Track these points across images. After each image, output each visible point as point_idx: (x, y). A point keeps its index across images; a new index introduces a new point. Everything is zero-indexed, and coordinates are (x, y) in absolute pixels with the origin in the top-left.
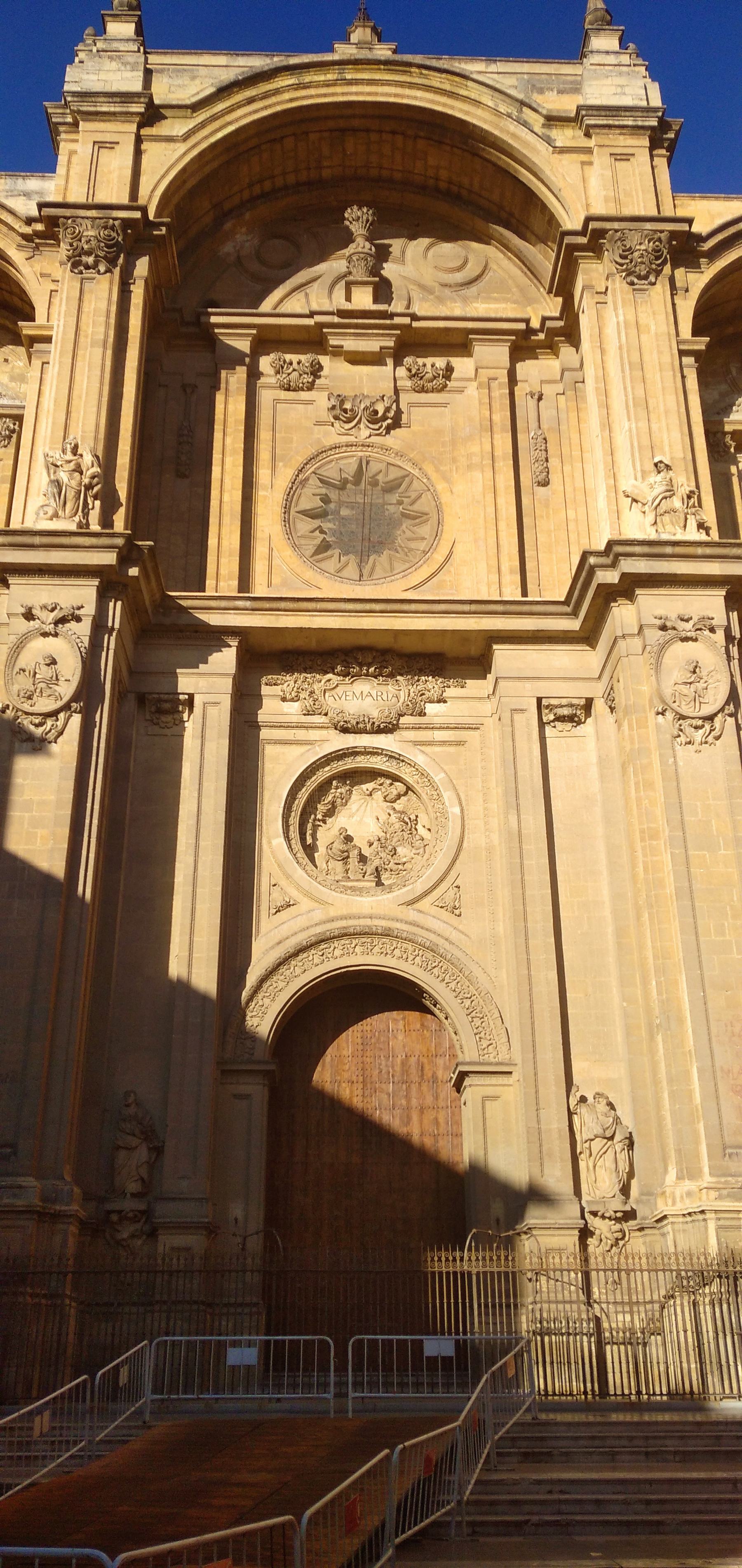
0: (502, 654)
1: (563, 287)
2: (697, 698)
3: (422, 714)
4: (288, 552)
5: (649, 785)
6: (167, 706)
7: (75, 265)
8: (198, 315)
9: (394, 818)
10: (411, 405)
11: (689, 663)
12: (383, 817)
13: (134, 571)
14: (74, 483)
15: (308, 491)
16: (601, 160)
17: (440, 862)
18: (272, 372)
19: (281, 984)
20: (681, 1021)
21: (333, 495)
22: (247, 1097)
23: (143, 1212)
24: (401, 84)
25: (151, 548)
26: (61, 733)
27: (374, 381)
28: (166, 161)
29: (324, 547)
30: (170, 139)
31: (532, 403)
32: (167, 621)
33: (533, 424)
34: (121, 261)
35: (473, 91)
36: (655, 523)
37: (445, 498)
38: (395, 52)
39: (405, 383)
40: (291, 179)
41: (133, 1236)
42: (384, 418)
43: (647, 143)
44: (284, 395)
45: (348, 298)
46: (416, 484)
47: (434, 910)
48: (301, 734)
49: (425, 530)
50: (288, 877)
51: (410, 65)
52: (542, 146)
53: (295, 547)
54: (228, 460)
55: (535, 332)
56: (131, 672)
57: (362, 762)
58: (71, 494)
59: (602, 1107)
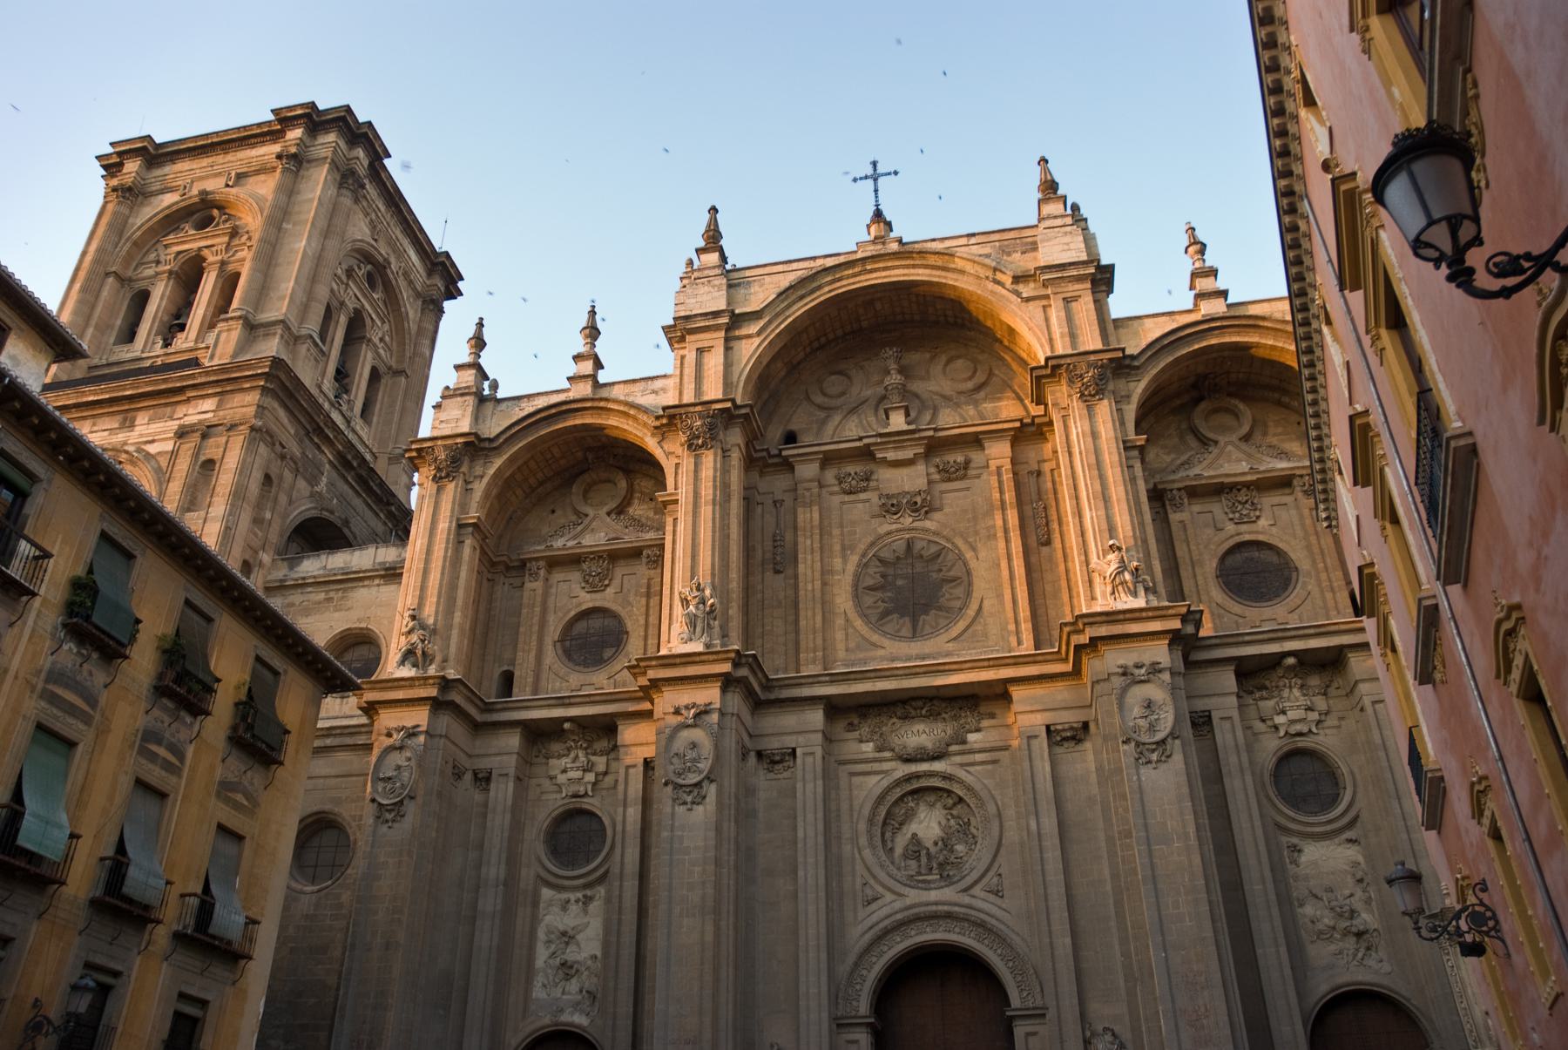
0: (1017, 692)
1: (1039, 400)
2: (1152, 728)
3: (964, 742)
4: (859, 623)
5: (1124, 797)
7: (690, 447)
9: (952, 822)
10: (942, 492)
12: (944, 822)
14: (699, 613)
15: (871, 571)
18: (835, 482)
20: (1151, 975)
21: (891, 571)
22: (856, 1042)
24: (907, 267)
25: (754, 656)
27: (912, 479)
29: (885, 614)
30: (749, 336)
31: (1033, 479)
32: (772, 696)
33: (1034, 497)
34: (721, 436)
35: (959, 264)
37: (973, 564)
39: (936, 477)
40: (840, 333)
44: (847, 498)
46: (950, 556)
47: (983, 894)
48: (876, 766)
49: (959, 591)
50: (874, 877)
52: (1013, 297)
53: (864, 616)
56: (751, 736)
57: (924, 783)
59: (1108, 1037)
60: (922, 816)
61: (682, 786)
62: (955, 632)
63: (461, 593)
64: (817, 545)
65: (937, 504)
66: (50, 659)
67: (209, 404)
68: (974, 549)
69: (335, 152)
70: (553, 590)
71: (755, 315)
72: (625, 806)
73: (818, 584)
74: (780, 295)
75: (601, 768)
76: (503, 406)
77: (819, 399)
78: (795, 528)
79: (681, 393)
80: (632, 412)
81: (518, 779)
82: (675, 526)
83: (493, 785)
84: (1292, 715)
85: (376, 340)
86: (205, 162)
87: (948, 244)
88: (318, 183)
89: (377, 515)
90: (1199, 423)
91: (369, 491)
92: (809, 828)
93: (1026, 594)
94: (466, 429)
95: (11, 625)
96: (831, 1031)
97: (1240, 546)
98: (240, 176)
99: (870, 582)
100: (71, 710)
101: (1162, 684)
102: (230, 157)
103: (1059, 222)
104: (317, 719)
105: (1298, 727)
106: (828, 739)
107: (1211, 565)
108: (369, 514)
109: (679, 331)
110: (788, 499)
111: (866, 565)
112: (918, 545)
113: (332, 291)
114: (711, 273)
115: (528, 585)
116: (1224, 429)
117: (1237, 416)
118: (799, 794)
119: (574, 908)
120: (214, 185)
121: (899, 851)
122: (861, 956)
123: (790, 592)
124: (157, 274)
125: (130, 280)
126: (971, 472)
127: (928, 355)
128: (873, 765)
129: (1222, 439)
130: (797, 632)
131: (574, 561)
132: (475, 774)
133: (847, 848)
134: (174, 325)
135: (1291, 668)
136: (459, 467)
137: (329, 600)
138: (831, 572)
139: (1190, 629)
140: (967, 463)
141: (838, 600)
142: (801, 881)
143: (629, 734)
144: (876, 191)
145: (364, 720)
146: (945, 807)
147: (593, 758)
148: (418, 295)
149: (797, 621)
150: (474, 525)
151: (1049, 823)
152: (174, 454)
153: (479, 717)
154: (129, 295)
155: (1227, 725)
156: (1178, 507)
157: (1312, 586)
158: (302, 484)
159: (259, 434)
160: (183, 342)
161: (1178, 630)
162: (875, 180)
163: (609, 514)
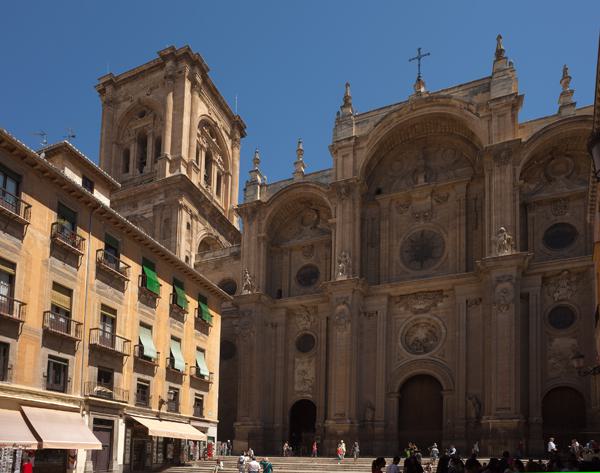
4: (401, 265)
37: (446, 239)
39: (434, 203)
62: (436, 266)
63: (261, 263)
67: (162, 197)
68: (447, 233)
78: (379, 230)
97: (556, 225)
100: (148, 315)
106: (388, 306)
107: (541, 234)
120: (142, 94)
128: (404, 316)
132: (272, 324)
150: (264, 238)
151: (463, 333)
158: (200, 225)
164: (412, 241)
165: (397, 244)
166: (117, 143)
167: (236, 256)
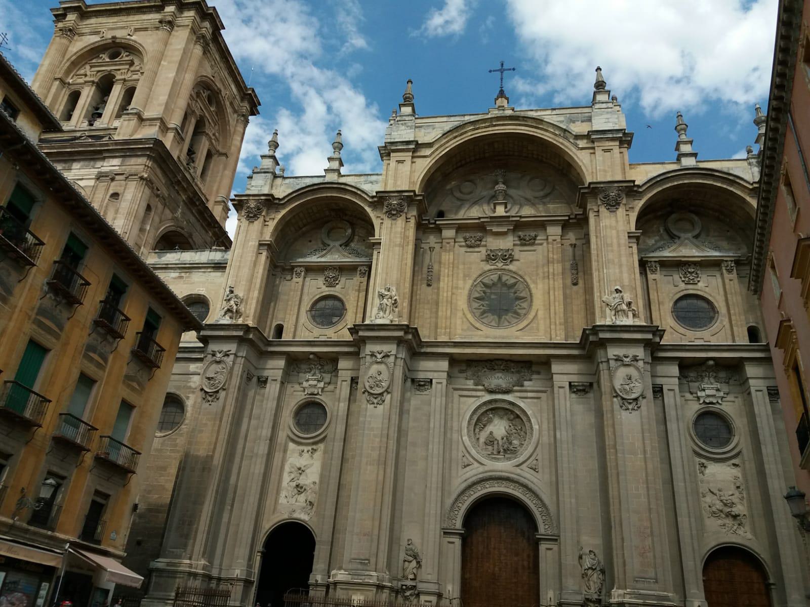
1: (583, 206)
3: (522, 386)
4: (469, 316)
6: (422, 383)
8: (436, 221)
10: (521, 251)
11: (627, 376)
12: (507, 427)
13: (410, 337)
16: (599, 152)
17: (530, 449)
19: (466, 498)
20: (621, 525)
21: (488, 291)
22: (453, 543)
23: (415, 586)
25: (416, 329)
26: (384, 401)
27: (507, 243)
28: (423, 166)
31: (570, 249)
32: (423, 350)
34: (406, 210)
36: (615, 315)
37: (534, 291)
38: (513, 110)
39: (518, 242)
40: (473, 158)
41: (411, 595)
42: (509, 258)
43: (617, 143)
45: (495, 208)
48: (474, 393)
49: (525, 305)
51: (519, 117)
54: (446, 279)
55: (572, 219)
58: (388, 307)
59: (592, 556)
60: (496, 422)
61: (373, 394)
63: (258, 281)
64: (451, 273)
65: (516, 257)
66: (40, 301)
67: (116, 162)
68: (535, 283)
69: (193, 22)
70: (307, 284)
71: (429, 145)
72: (339, 401)
73: (450, 293)
74: (443, 135)
75: (327, 380)
76: (287, 181)
77: (458, 195)
78: (440, 263)
79: (386, 185)
80: (359, 192)
81: (282, 383)
82: (378, 256)
83: (268, 385)
84: (708, 392)
85: (211, 135)
86: (115, 19)
87: (539, 113)
88: (181, 38)
89: (207, 232)
90: (670, 225)
91: (204, 219)
92: (436, 422)
93: (562, 310)
94: (266, 192)
95: (20, 281)
96: (440, 536)
98: (136, 30)
99: (477, 295)
101: (637, 369)
102: (131, 18)
103: (604, 106)
104: (179, 342)
105: (711, 399)
106: (450, 376)
107: (668, 305)
108: (204, 232)
109: (387, 151)
110: (437, 246)
111: (475, 286)
112: (504, 278)
113: (188, 104)
114: (407, 118)
115: (295, 280)
116: (686, 231)
117: (693, 226)
118: (433, 403)
119: (306, 455)
120: (120, 34)
121: (482, 440)
122: (459, 496)
123: (435, 297)
124: (86, 82)
125: (69, 84)
126: (536, 242)
127: (520, 175)
129: (682, 235)
130: (437, 318)
131: (319, 269)
132: (259, 378)
133: (455, 436)
134: (95, 114)
135: (712, 366)
136: (262, 212)
137: (181, 277)
138: (457, 288)
139: (657, 339)
140: (536, 236)
141: (460, 303)
142: (430, 451)
143: (343, 364)
144: (502, 79)
145: (201, 345)
146: (509, 419)
147: (324, 375)
148: (235, 111)
149: (437, 312)
150: (268, 245)
152: (94, 188)
153: (264, 348)
154: (68, 93)
155: (671, 393)
156: (654, 272)
157: (726, 322)
158: (167, 212)
159: (148, 182)
160: (98, 124)
161: (651, 339)
162: (502, 73)
163: (341, 246)
164: (485, 285)
165: (464, 287)
166: (61, 80)
167: (219, 267)
